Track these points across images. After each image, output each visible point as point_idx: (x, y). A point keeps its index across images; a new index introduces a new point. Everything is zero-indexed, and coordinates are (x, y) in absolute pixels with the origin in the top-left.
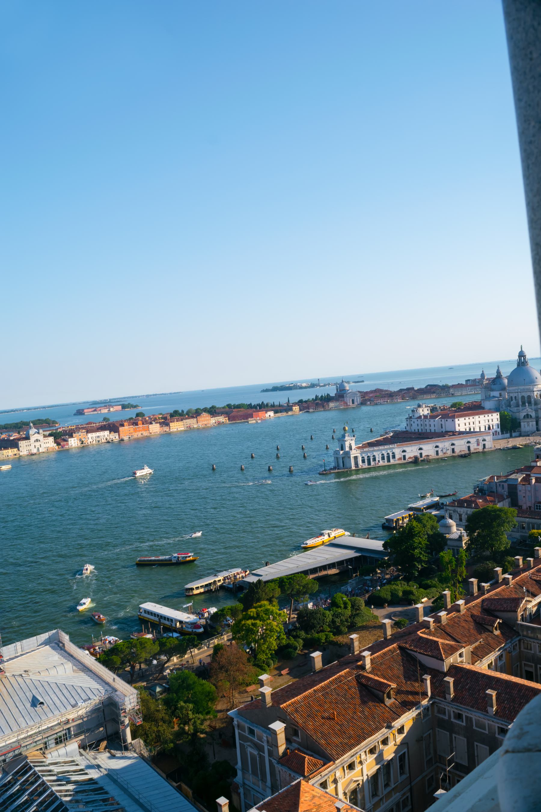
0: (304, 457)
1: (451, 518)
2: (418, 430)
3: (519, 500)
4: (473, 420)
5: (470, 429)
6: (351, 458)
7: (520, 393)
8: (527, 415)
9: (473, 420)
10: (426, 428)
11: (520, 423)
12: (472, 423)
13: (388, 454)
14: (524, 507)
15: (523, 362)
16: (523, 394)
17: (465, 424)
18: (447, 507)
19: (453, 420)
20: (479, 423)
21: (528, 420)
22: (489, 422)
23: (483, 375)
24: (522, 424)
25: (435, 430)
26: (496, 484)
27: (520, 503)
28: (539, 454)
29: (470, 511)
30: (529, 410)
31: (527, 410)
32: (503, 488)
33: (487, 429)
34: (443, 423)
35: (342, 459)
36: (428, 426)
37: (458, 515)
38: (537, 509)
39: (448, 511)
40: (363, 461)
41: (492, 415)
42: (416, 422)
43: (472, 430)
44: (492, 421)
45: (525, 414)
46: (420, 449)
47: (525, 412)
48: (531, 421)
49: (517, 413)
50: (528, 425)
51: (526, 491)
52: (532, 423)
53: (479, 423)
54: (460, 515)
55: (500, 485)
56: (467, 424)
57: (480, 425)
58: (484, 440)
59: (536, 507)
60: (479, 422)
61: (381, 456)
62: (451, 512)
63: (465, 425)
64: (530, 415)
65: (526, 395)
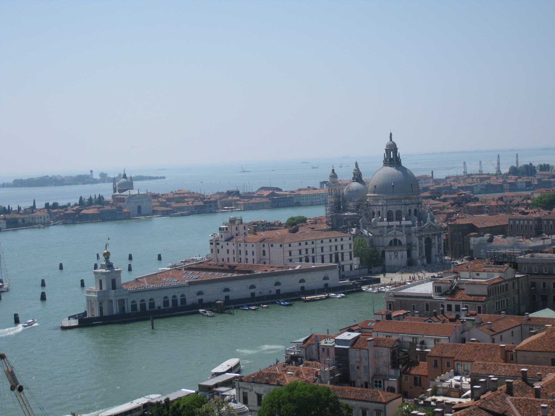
0: (43, 297)
2: (228, 259)
3: (351, 373)
4: (314, 246)
6: (114, 302)
7: (385, 207)
8: (395, 240)
9: (314, 246)
10: (240, 256)
11: (383, 252)
12: (310, 251)
13: (174, 296)
14: (359, 383)
15: (391, 160)
16: (391, 208)
17: (300, 251)
18: (242, 384)
19: (281, 246)
20: (322, 251)
21: (396, 248)
22: (336, 249)
23: (334, 175)
24: (387, 254)
25: (253, 260)
26: (318, 348)
27: (353, 377)
28: (393, 302)
31: (395, 233)
32: (328, 355)
35: (100, 303)
36: (243, 253)
37: (256, 397)
38: (376, 386)
39: (241, 390)
40: (134, 307)
41: (342, 240)
42: (226, 247)
44: (342, 249)
45: (392, 238)
46: (227, 290)
47: (392, 236)
48: (401, 250)
49: (380, 238)
50: (396, 256)
51: (361, 359)
52: (390, 253)
53: (322, 251)
54: (259, 397)
55: (323, 349)
56: (303, 252)
57: (323, 254)
59: (375, 384)
60: (322, 248)
61: (162, 300)
62: (245, 391)
63: (300, 253)
64: (400, 242)
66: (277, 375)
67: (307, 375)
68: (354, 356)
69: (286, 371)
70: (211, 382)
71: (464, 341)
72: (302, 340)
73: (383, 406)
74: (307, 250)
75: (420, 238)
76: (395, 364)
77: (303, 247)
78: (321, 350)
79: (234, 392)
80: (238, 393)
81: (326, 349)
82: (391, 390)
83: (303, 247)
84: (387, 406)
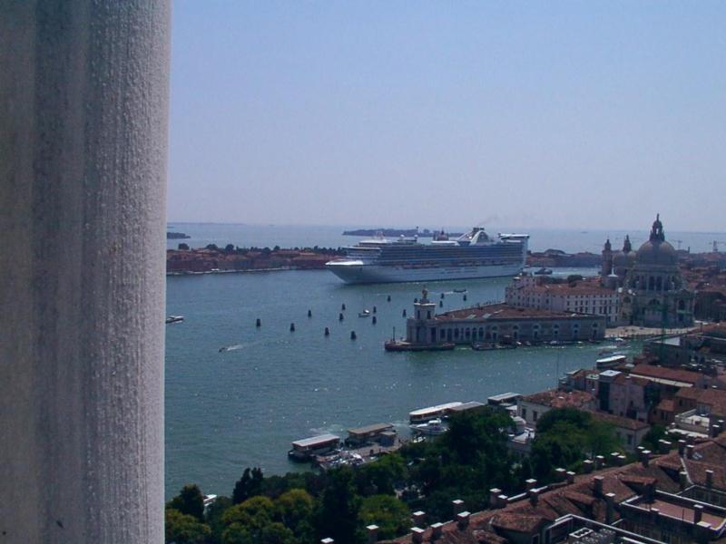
1: (524, 417)
5: (581, 310)
12: (584, 303)
15: (657, 236)
18: (523, 403)
23: (608, 245)
24: (646, 312)
27: (611, 408)
29: (546, 410)
30: (658, 295)
33: (603, 311)
34: (549, 298)
36: (531, 300)
43: (584, 312)
45: (651, 299)
54: (535, 414)
56: (579, 303)
58: (595, 325)
65: (656, 275)
66: (552, 399)
67: (575, 401)
68: (614, 392)
69: (558, 396)
70: (497, 398)
71: (706, 387)
72: (573, 373)
73: (633, 432)
74: (582, 302)
75: (675, 300)
76: (646, 399)
77: (579, 299)
78: (587, 383)
79: (514, 408)
80: (519, 408)
81: (592, 382)
82: (641, 420)
83: (579, 299)
84: (638, 434)
